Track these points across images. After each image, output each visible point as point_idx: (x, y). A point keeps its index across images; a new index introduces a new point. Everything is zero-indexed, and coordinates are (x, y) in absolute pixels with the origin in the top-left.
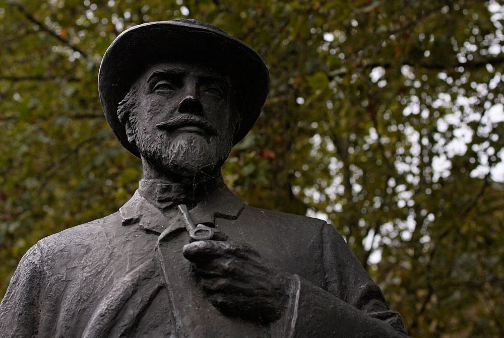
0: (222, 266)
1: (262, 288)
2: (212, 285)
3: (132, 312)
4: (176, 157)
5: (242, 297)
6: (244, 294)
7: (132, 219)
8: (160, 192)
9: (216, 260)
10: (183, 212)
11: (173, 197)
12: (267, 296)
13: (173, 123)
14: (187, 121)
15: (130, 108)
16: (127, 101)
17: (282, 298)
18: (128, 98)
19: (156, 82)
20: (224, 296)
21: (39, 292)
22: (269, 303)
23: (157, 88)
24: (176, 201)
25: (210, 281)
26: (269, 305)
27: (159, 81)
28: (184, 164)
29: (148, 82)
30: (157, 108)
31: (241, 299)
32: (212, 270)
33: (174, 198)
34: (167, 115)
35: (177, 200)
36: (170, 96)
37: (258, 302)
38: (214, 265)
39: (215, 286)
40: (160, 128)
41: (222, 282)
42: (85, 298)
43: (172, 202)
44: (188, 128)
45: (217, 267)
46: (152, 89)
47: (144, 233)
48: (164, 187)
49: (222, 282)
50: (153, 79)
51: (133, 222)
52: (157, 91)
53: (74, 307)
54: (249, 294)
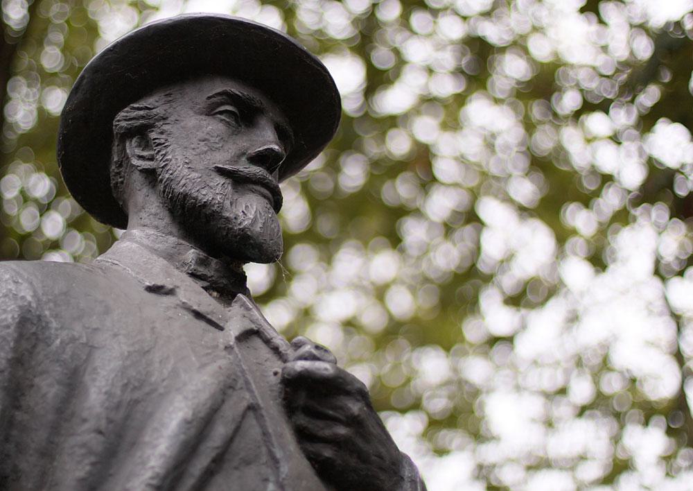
0: (349, 409)
1: (381, 457)
2: (322, 429)
3: (220, 431)
4: (252, 224)
5: (354, 460)
6: (359, 457)
7: (162, 287)
8: (196, 262)
9: (342, 397)
10: (251, 307)
11: (212, 276)
12: (381, 469)
13: (248, 174)
14: (266, 179)
15: (158, 120)
16: (154, 108)
17: (395, 478)
18: (155, 103)
19: (222, 104)
20: (336, 451)
21: (34, 346)
22: (380, 480)
23: (221, 113)
24: (213, 283)
25: (320, 423)
26: (379, 482)
27: (228, 104)
28: (261, 239)
29: (209, 98)
30: (217, 141)
31: (353, 462)
32: (332, 409)
33: (214, 278)
34: (232, 157)
35: (215, 283)
36: (235, 132)
37: (369, 473)
38: (339, 403)
39: (327, 432)
40: (221, 172)
41: (342, 431)
42: (137, 384)
43: (209, 284)
44: (258, 188)
45: (341, 408)
46: (212, 110)
47: (188, 317)
48: (201, 256)
49: (342, 431)
50: (220, 98)
51: (163, 291)
52: (219, 116)
53: (119, 392)
54: (362, 457)
